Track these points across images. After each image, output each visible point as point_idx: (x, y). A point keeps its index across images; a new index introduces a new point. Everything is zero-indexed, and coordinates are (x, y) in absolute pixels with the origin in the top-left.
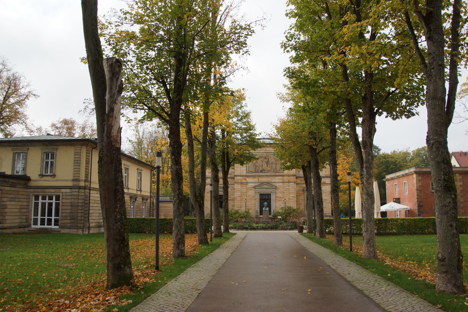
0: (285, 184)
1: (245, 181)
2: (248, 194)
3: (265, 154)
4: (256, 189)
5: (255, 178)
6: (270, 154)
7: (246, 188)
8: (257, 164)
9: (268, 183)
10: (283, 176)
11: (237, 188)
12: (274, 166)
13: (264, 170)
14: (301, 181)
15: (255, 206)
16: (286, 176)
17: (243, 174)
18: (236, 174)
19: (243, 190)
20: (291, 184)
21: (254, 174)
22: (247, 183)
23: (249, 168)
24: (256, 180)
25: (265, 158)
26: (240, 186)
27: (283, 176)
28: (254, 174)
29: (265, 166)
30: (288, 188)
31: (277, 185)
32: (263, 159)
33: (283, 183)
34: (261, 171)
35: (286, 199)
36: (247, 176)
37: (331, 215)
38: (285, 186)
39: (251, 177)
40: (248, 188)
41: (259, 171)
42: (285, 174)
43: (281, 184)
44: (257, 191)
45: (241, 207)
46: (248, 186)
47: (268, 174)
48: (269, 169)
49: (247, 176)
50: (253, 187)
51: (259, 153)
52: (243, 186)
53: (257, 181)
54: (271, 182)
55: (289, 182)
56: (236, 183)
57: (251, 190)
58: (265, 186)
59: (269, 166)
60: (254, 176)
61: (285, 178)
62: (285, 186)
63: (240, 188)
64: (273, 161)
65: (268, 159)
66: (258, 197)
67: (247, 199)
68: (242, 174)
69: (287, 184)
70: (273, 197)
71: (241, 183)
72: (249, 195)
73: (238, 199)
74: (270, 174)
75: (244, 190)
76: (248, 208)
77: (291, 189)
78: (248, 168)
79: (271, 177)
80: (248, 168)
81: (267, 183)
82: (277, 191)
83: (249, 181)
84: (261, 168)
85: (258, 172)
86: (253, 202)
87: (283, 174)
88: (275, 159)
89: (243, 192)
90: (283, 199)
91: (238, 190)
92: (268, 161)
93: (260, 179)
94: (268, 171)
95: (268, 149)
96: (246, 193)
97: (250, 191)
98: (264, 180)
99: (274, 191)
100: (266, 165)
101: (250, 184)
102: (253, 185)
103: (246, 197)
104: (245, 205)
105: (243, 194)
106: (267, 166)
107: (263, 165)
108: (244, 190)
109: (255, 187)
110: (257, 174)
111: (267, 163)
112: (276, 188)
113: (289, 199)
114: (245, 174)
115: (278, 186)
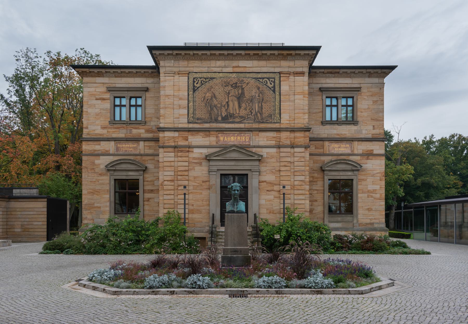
0: (282, 150)
1: (186, 143)
2: (192, 174)
3: (234, 75)
4: (211, 163)
5: (209, 136)
6: (248, 75)
7: (186, 159)
8: (215, 102)
9: (241, 148)
10: (278, 130)
11: (166, 159)
12: (256, 106)
13: (232, 116)
14: (316, 148)
15: (209, 205)
16: (286, 130)
17: (180, 126)
18: (162, 125)
19: (180, 164)
20: (296, 150)
21: (207, 125)
22: (189, 147)
23: (194, 110)
24: (212, 140)
25: (235, 86)
26: (172, 154)
27: (278, 130)
28: (207, 125)
29: (234, 106)
30: (289, 159)
31: (264, 152)
32: (230, 88)
33: (279, 147)
34: (225, 119)
35: (287, 187)
36: (189, 130)
37: (384, 226)
38: (282, 154)
39: (201, 134)
40: (191, 160)
41: (220, 118)
42: (282, 126)
43: (274, 150)
44: (215, 168)
45: (176, 204)
46: (191, 155)
47: (242, 126)
48: (243, 112)
49: (189, 130)
50: (204, 156)
51: (221, 75)
52: (180, 154)
53: (214, 143)
54: (249, 146)
55: (292, 147)
56: (163, 147)
57: (200, 164)
58: (234, 155)
59: (243, 105)
60: (207, 131)
61: (284, 135)
62: (282, 154)
63: (172, 159)
64: (253, 94)
65: (243, 89)
66: (216, 181)
67: (191, 188)
68: (176, 126)
69: (289, 150)
70: (253, 182)
71: (175, 147)
72: (195, 178)
73: (169, 186)
74: (247, 126)
75: (182, 165)
76: (191, 207)
77: (296, 164)
78: (191, 111)
79: (248, 135)
80: (191, 111)
81: (241, 148)
82: (263, 169)
83: (194, 144)
84: (223, 110)
85: (216, 121)
86: (205, 193)
87: (277, 126)
88: (259, 88)
89: (180, 169)
90: (276, 188)
91: (168, 164)
92: (243, 93)
93: (222, 139)
94: (243, 119)
95: (242, 63)
96: (186, 173)
97: (197, 168)
98: (232, 139)
99: (256, 168)
100: (236, 104)
101: (196, 150)
102: (205, 151)
103: (186, 183)
104: (182, 202)
105: (179, 173)
106: (240, 107)
107: (231, 104)
108: (182, 165)
109: (208, 158)
110: (214, 125)
111: (240, 98)
112: (260, 159)
113: (293, 187)
114: (186, 126)
115: (265, 155)
